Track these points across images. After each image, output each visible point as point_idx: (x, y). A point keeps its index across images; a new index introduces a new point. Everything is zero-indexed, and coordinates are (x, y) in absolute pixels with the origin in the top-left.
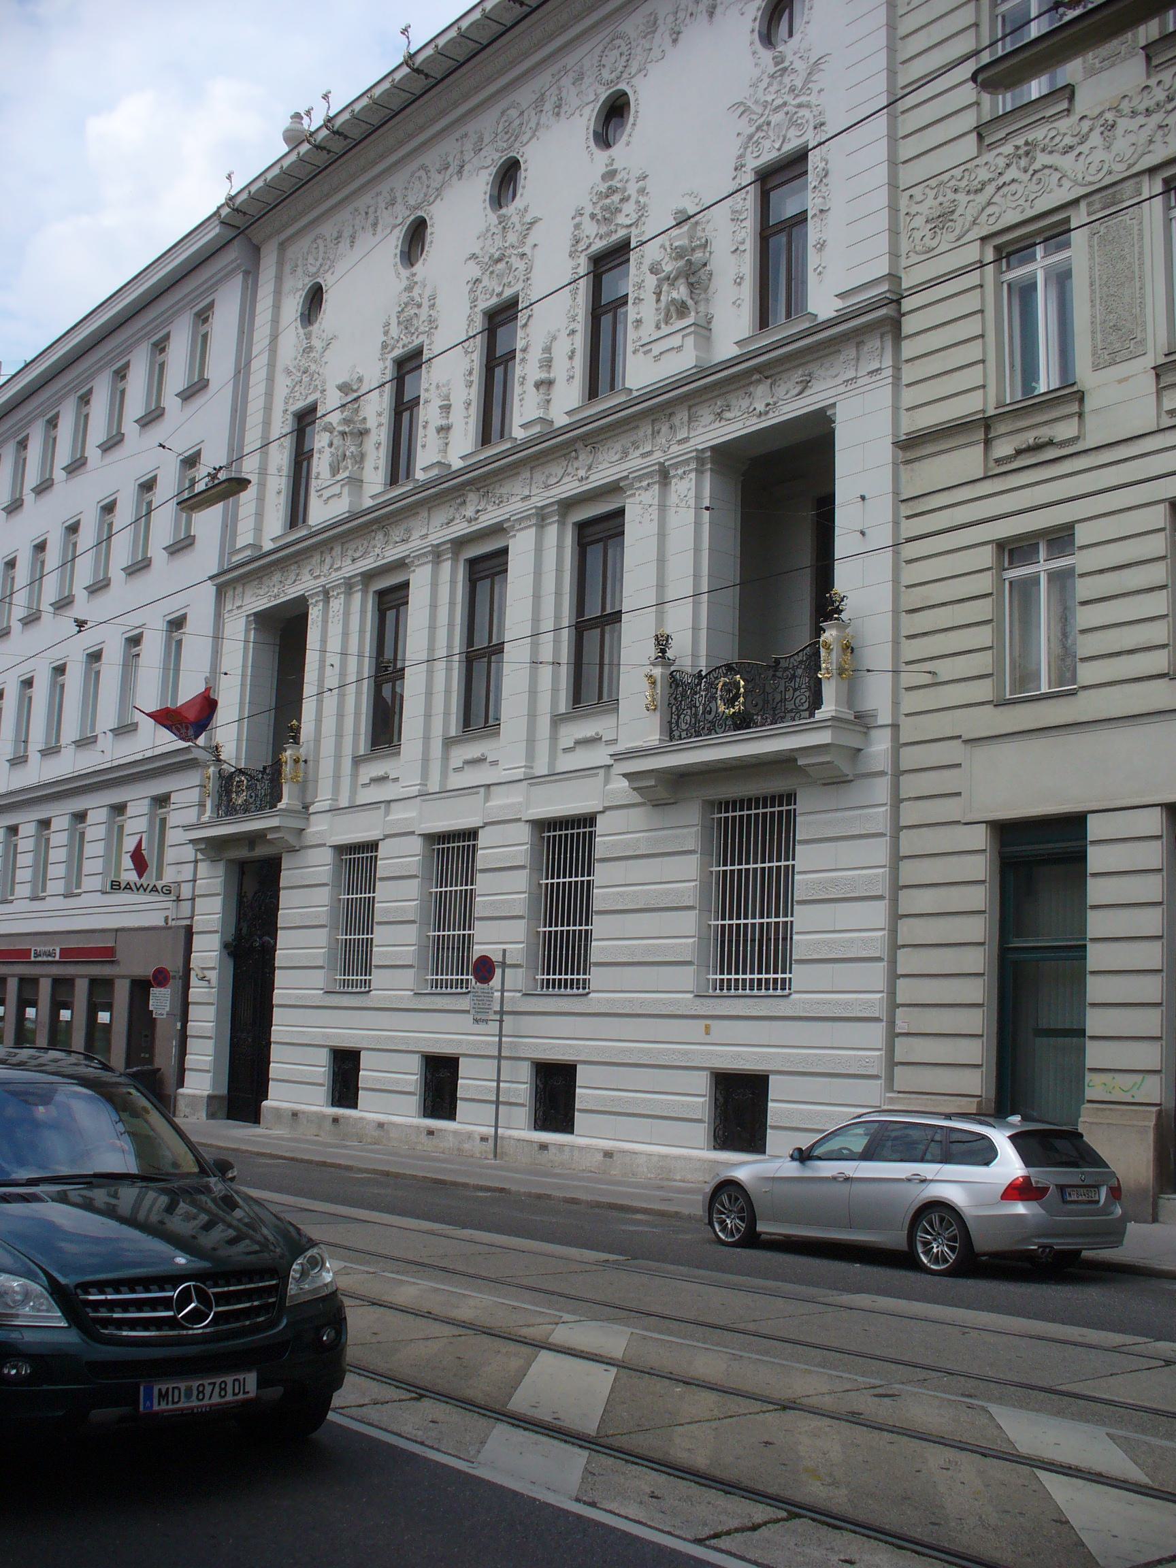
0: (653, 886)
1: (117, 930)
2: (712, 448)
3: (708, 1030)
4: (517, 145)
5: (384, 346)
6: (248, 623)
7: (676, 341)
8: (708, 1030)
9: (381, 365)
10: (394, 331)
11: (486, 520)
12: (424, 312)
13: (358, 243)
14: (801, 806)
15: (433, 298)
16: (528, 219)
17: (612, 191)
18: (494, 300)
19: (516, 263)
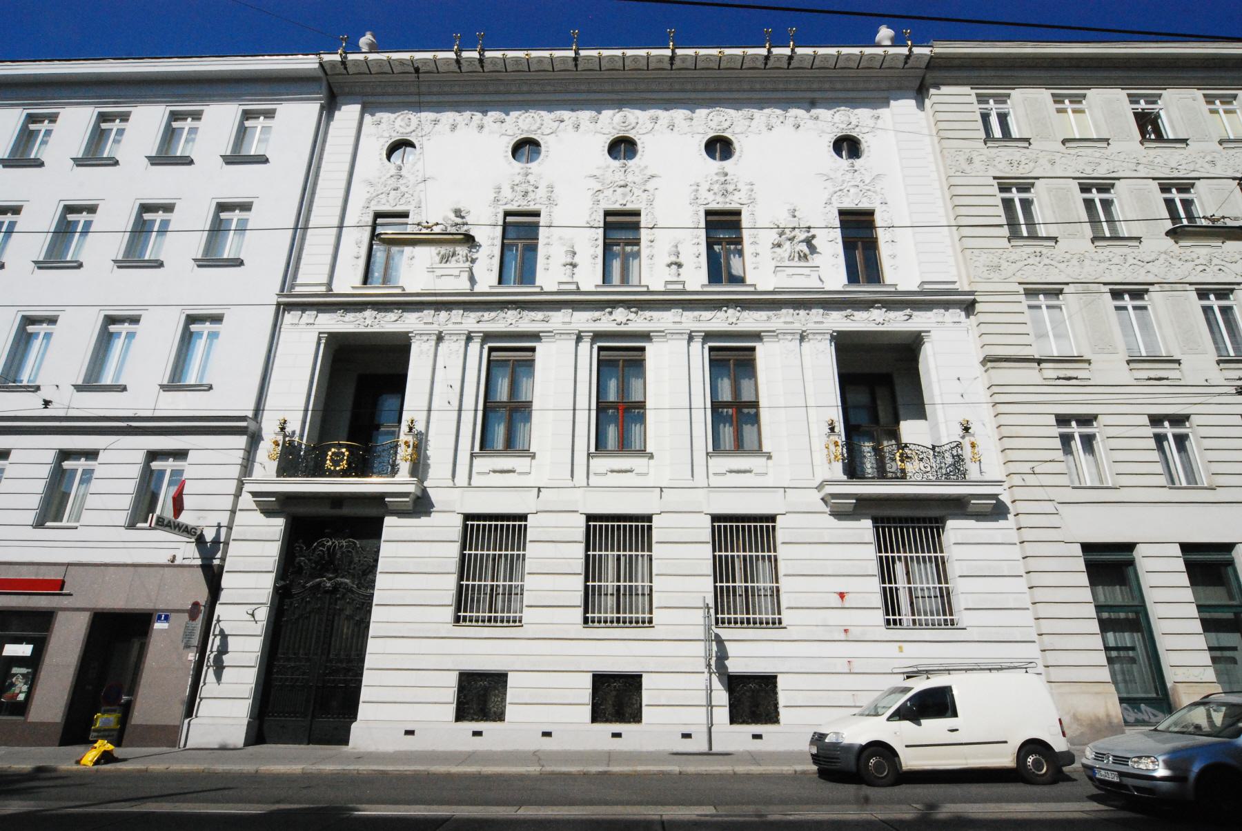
0: (827, 561)
1: (69, 564)
2: (838, 332)
3: (901, 649)
4: (634, 132)
5: (497, 200)
6: (319, 339)
7: (807, 271)
8: (901, 649)
9: (492, 209)
10: (507, 193)
11: (632, 327)
12: (542, 192)
13: (457, 131)
14: (950, 524)
15: (551, 188)
16: (649, 172)
17: (725, 182)
18: (617, 207)
19: (637, 192)
